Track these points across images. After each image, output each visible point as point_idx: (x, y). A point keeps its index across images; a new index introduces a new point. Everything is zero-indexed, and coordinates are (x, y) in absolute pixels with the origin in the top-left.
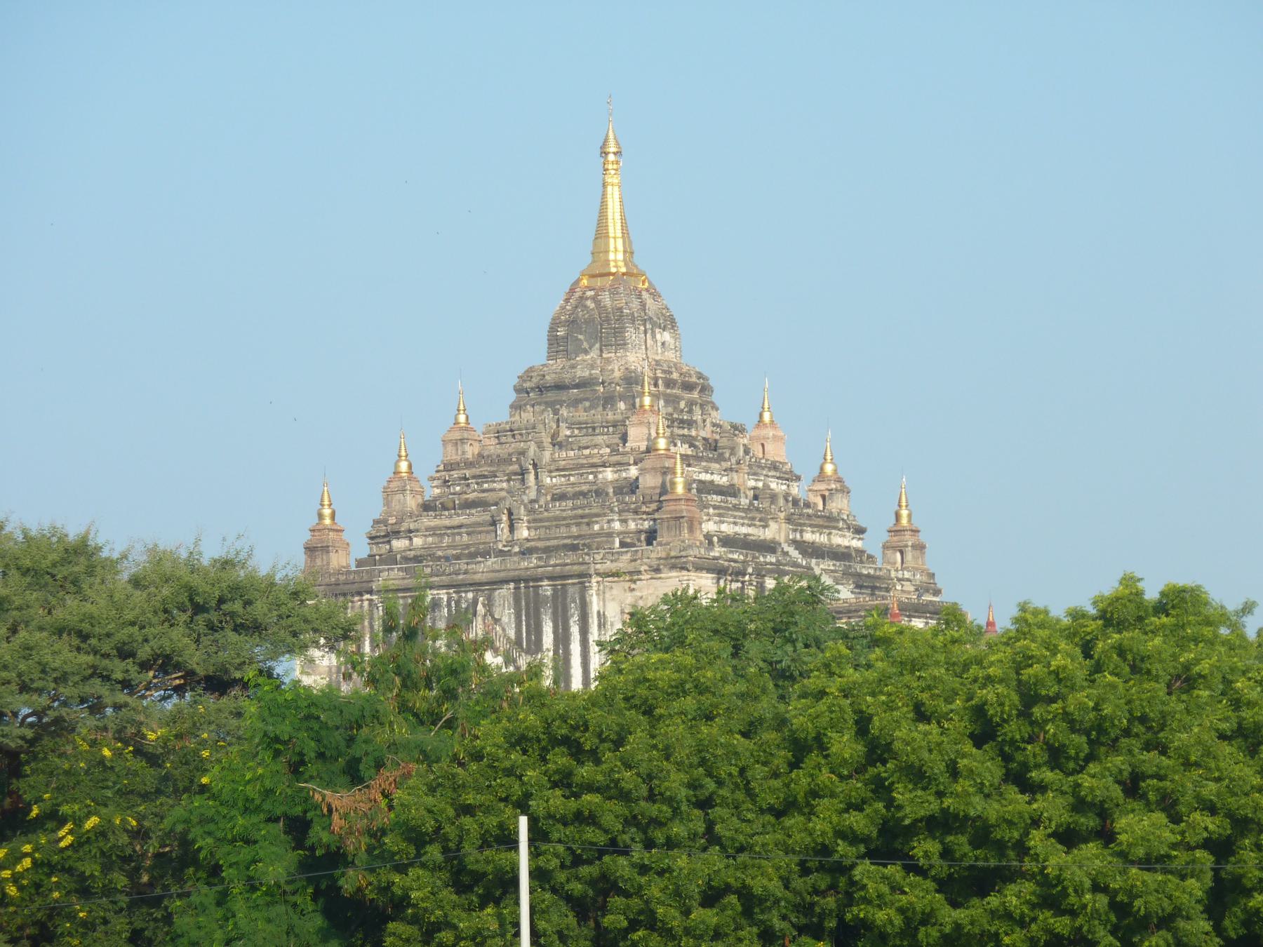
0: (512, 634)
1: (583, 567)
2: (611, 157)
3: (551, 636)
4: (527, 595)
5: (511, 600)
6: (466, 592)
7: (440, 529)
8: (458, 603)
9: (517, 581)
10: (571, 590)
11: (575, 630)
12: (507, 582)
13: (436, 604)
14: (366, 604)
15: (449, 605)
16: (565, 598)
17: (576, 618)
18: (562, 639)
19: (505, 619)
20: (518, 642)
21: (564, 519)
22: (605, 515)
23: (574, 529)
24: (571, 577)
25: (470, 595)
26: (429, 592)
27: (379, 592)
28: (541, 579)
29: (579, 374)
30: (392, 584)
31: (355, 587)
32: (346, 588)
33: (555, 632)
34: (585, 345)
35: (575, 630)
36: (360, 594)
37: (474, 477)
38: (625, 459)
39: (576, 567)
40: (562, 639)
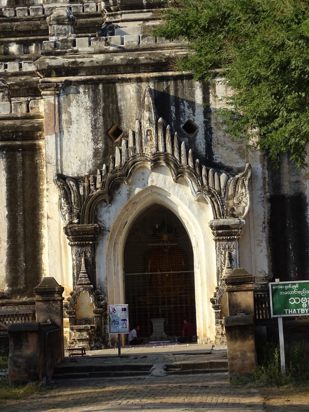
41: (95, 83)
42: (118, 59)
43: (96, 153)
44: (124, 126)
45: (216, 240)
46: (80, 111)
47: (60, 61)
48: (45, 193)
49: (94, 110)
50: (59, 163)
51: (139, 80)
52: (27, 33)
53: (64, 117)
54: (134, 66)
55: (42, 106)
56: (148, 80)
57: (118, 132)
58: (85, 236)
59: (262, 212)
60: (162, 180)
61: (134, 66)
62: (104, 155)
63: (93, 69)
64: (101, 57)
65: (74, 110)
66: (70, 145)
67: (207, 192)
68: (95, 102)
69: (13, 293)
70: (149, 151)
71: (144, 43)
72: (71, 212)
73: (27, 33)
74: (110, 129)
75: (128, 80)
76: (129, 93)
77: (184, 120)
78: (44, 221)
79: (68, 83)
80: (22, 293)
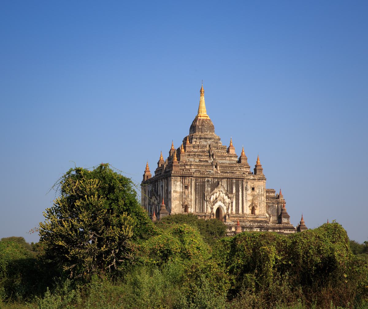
0: (226, 189)
1: (243, 177)
2: (203, 93)
3: (235, 191)
4: (230, 181)
5: (226, 182)
6: (215, 179)
7: (198, 165)
9: (227, 178)
10: (239, 181)
11: (240, 190)
12: (225, 178)
13: (208, 181)
14: (190, 179)
15: (211, 181)
16: (238, 183)
17: (241, 187)
18: (237, 191)
19: (224, 186)
20: (227, 191)
21: (228, 166)
22: (237, 167)
23: (230, 169)
25: (216, 180)
26: (206, 178)
27: (195, 177)
28: (233, 179)
29: (209, 136)
30: (198, 176)
31: (188, 175)
32: (186, 175)
33: (236, 190)
34: (206, 130)
35: (240, 190)
36: (189, 177)
37: (197, 155)
38: (232, 156)
39: (241, 177)
40: (237, 191)
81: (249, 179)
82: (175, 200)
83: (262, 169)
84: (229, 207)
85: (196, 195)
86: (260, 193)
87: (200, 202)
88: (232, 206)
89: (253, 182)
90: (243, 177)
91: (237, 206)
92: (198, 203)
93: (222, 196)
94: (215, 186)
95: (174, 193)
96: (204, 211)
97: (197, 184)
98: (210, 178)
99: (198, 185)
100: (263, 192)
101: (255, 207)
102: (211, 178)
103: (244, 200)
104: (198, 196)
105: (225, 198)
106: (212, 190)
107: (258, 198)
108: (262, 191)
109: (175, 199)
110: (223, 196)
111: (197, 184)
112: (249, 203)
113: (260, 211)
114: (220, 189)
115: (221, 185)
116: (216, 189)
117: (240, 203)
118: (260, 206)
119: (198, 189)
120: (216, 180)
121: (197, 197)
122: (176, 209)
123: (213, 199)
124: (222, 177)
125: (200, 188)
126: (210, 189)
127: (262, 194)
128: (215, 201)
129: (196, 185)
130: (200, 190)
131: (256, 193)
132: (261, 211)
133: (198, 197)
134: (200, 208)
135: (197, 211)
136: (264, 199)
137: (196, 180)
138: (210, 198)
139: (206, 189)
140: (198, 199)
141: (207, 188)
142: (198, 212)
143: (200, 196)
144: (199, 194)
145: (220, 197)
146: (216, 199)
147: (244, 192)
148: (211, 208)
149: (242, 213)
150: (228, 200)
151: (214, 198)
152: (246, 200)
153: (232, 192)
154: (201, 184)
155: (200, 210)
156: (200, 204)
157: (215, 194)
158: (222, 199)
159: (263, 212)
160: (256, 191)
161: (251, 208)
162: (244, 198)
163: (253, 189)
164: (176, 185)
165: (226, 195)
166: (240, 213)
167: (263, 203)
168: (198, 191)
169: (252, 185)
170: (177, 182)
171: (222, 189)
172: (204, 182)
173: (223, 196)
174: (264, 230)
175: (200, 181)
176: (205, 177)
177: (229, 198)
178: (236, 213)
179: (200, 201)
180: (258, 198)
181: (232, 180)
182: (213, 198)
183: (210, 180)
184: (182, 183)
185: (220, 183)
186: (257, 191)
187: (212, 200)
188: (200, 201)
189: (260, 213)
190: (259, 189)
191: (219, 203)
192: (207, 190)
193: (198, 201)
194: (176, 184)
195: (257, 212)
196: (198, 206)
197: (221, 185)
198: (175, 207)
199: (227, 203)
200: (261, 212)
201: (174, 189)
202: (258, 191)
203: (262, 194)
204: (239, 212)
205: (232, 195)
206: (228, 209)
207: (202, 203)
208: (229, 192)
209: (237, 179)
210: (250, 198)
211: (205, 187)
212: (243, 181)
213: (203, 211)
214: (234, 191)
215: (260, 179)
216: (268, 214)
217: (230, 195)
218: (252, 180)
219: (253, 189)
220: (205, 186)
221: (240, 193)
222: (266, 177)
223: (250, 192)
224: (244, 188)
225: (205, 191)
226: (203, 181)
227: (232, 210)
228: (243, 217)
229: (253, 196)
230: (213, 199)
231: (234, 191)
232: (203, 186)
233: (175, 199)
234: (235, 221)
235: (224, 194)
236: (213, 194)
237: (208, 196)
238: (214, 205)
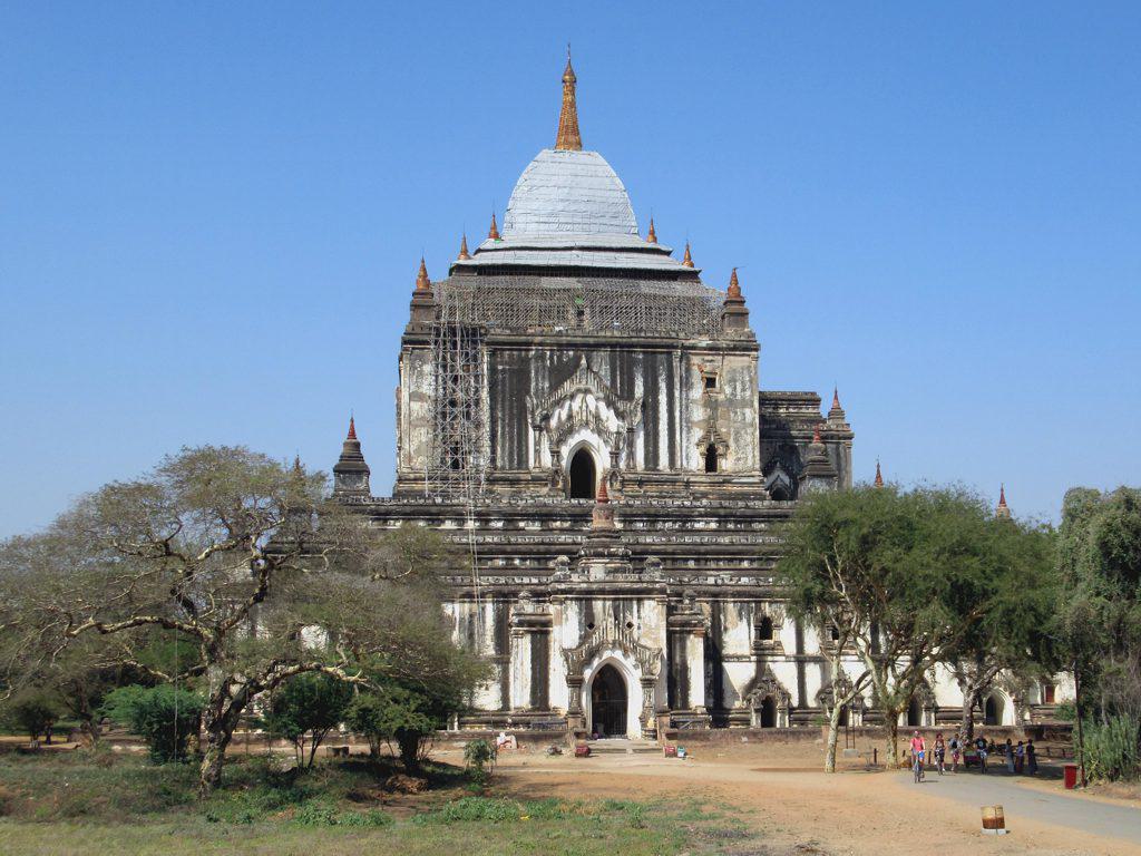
3: (642, 389)
8: (559, 358)
9: (613, 346)
11: (663, 386)
12: (604, 345)
13: (541, 357)
17: (663, 377)
24: (662, 347)
35: (663, 386)
40: (652, 390)
41: (581, 599)
42: (595, 586)
43: (580, 637)
44: (596, 623)
45: (643, 688)
46: (573, 610)
47: (563, 586)
48: (552, 656)
49: (580, 614)
50: (561, 641)
51: (604, 599)
52: (525, 553)
53: (564, 616)
54: (602, 592)
55: (552, 609)
56: (609, 599)
57: (591, 626)
58: (575, 682)
59: (665, 673)
60: (618, 654)
61: (602, 592)
62: (584, 639)
63: (580, 592)
64: (584, 586)
65: (569, 612)
66: (566, 632)
67: (641, 663)
68: (580, 609)
69: (533, 710)
70: (610, 639)
71: (607, 579)
72: (569, 669)
73: (525, 553)
74: (589, 623)
75: (599, 599)
76: (598, 606)
77: (627, 622)
78: (551, 671)
79: (566, 599)
80: (538, 709)
81: (694, 348)
82: (416, 426)
83: (745, 314)
84: (617, 448)
85: (493, 409)
86: (739, 397)
87: (511, 432)
88: (631, 444)
89: (710, 358)
90: (671, 341)
91: (651, 442)
92: (503, 434)
93: (592, 408)
94: (561, 374)
95: (412, 403)
96: (527, 462)
97: (500, 367)
98: (548, 345)
99: (503, 370)
100: (748, 393)
101: (721, 450)
102: (551, 345)
103: (677, 420)
104: (503, 410)
105: (604, 417)
106: (555, 387)
107: (732, 415)
108: (743, 390)
109: (419, 423)
110: (597, 407)
111: (500, 367)
112: (698, 433)
113: (739, 459)
114: (582, 386)
115: (589, 368)
116: (567, 385)
117: (661, 434)
118: (736, 440)
119: (504, 385)
120: (571, 353)
121: (500, 415)
122: (421, 459)
123: (559, 418)
124: (591, 341)
125: (511, 383)
126: (547, 385)
127: (743, 399)
128: (567, 430)
129: (493, 370)
130: (511, 390)
131: (721, 397)
132: (743, 457)
133: (504, 416)
134: (511, 454)
135: (499, 464)
136: (754, 419)
137: (493, 354)
138: (546, 418)
139: (533, 385)
140: (503, 420)
141: (537, 380)
142: (503, 468)
143: (511, 408)
144: (507, 403)
145: (584, 414)
146: (570, 417)
147: (677, 394)
148: (552, 452)
149: (671, 469)
150: (613, 423)
151: (564, 417)
152: (688, 421)
153: (630, 396)
154: (516, 367)
155: (511, 461)
156: (511, 438)
157: (567, 404)
158: (591, 418)
159: (750, 463)
160: (722, 391)
161: (703, 449)
162: (677, 414)
163: (710, 382)
164: (421, 374)
165: (610, 404)
166: (661, 467)
167: (749, 430)
168: (503, 392)
169: (708, 368)
170: (424, 363)
171: (593, 386)
172: (526, 361)
173: (597, 407)
174: (736, 522)
175: (511, 356)
176: (530, 344)
177: (620, 415)
178: (646, 469)
179: (511, 427)
180: (732, 415)
181: (632, 352)
182: (561, 414)
183: (548, 353)
184: (445, 367)
185: (584, 361)
186: (724, 391)
187: (553, 423)
188: (511, 427)
189: (740, 466)
190: (735, 381)
191: (585, 435)
192: (537, 390)
193: (503, 428)
194: (422, 371)
195: (726, 465)
196: (503, 446)
197: (589, 368)
198: (418, 451)
199: (612, 434)
200: (742, 462)
201: (413, 388)
202: (728, 390)
203: (743, 399)
204: (658, 465)
205: (629, 406)
206: (615, 455)
207: (519, 434)
208: (618, 395)
209: (651, 349)
210: (698, 414)
211: (529, 379)
212: (670, 353)
213: (522, 461)
214: (639, 391)
215: (735, 348)
216: (787, 474)
217: (621, 406)
218: (705, 349)
219: (710, 382)
220: (530, 372)
221: (663, 398)
222: (759, 339)
223: (698, 391)
224: (677, 380)
225: (528, 392)
226: (519, 356)
227: (631, 455)
228: (674, 482)
229: (710, 404)
230: (559, 418)
231: (639, 391)
232: (521, 376)
233: (419, 423)
234: (638, 496)
235: (602, 405)
236: (559, 403)
237: (540, 410)
238: (560, 441)
